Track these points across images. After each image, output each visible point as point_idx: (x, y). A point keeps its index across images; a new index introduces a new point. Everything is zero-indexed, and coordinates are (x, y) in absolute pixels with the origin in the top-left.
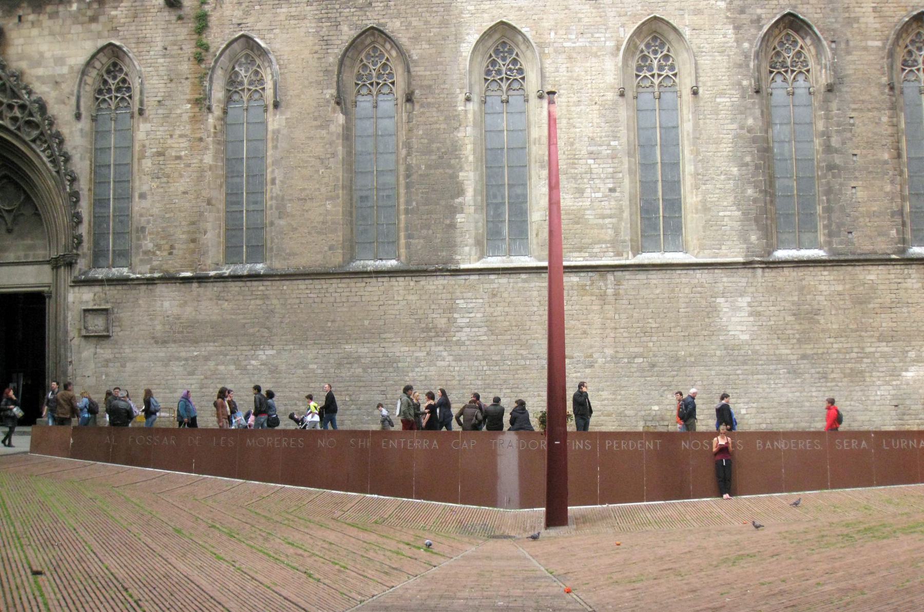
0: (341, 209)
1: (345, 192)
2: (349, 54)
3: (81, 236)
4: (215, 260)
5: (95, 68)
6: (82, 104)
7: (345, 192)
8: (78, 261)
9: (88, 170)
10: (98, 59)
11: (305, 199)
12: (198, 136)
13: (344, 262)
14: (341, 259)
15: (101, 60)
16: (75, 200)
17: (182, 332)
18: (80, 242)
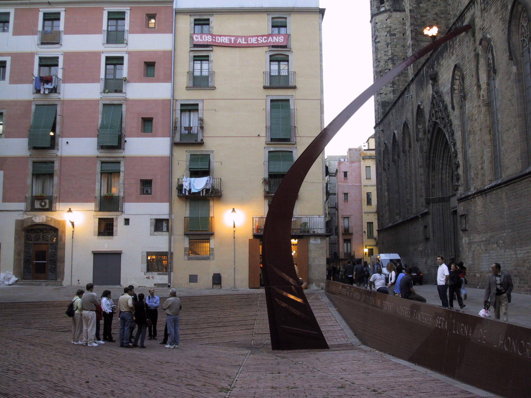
0: (518, 131)
1: (520, 119)
2: (513, 23)
3: (458, 175)
4: (490, 178)
5: (457, 79)
6: (454, 101)
7: (520, 119)
8: (459, 189)
9: (461, 137)
10: (456, 75)
11: (508, 130)
12: (479, 104)
13: (522, 167)
14: (521, 167)
15: (458, 74)
16: (454, 155)
17: (483, 225)
18: (458, 179)
